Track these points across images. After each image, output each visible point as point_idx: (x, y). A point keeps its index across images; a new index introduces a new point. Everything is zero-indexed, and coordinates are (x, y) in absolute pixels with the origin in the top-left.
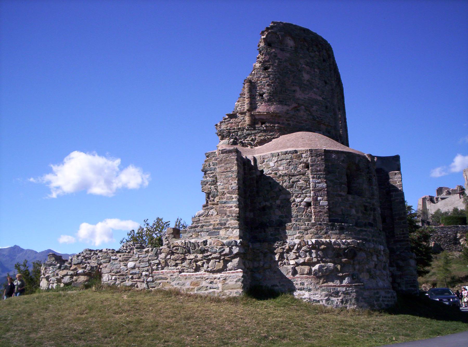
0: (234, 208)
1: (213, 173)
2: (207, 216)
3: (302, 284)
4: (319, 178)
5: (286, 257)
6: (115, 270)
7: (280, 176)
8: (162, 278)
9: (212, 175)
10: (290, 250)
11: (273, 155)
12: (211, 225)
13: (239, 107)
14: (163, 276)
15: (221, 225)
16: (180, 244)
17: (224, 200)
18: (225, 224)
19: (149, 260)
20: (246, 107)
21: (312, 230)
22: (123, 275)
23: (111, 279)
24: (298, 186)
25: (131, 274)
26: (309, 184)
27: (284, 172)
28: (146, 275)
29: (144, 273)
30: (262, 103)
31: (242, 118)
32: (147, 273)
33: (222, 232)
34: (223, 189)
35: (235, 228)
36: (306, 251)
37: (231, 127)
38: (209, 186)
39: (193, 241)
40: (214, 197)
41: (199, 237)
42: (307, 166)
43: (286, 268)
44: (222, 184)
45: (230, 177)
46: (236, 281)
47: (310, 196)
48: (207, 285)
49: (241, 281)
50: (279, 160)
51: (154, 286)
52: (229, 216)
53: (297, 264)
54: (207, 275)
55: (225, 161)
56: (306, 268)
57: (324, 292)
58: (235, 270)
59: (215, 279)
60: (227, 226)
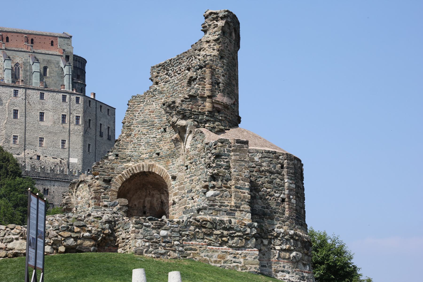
0: (246, 194)
1: (227, 159)
2: (222, 197)
3: (284, 267)
4: (291, 180)
5: (273, 243)
6: (148, 237)
7: (263, 171)
8: (191, 249)
9: (226, 160)
10: (277, 237)
11: (257, 151)
12: (228, 206)
13: (200, 91)
14: (193, 247)
15: (237, 208)
16: (209, 219)
17: (239, 186)
18: (239, 208)
19: (180, 231)
20: (207, 93)
21: (287, 223)
22: (156, 242)
23: (144, 246)
24: (276, 183)
25: (164, 242)
26: (284, 183)
27: (266, 168)
28: (177, 245)
29: (176, 243)
30: (219, 93)
31: (202, 102)
32: (178, 243)
33: (237, 214)
34: (238, 175)
35: (248, 212)
36: (287, 240)
37: (192, 108)
38: (224, 170)
39: (218, 218)
40: (227, 180)
41: (218, 215)
42: (282, 167)
43: (273, 252)
44: (237, 171)
45: (243, 165)
46: (254, 258)
47: (284, 194)
48: (232, 259)
49: (258, 258)
50: (263, 156)
51: (186, 255)
52: (242, 201)
53: (282, 250)
54: (231, 250)
55: (240, 150)
56: (287, 255)
57: (297, 276)
58: (253, 248)
59: (237, 254)
60: (242, 209)
